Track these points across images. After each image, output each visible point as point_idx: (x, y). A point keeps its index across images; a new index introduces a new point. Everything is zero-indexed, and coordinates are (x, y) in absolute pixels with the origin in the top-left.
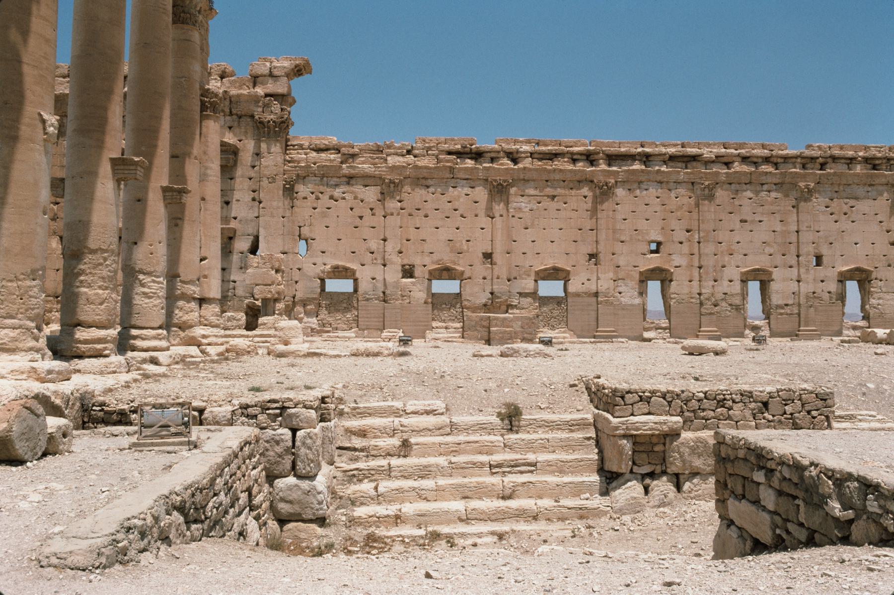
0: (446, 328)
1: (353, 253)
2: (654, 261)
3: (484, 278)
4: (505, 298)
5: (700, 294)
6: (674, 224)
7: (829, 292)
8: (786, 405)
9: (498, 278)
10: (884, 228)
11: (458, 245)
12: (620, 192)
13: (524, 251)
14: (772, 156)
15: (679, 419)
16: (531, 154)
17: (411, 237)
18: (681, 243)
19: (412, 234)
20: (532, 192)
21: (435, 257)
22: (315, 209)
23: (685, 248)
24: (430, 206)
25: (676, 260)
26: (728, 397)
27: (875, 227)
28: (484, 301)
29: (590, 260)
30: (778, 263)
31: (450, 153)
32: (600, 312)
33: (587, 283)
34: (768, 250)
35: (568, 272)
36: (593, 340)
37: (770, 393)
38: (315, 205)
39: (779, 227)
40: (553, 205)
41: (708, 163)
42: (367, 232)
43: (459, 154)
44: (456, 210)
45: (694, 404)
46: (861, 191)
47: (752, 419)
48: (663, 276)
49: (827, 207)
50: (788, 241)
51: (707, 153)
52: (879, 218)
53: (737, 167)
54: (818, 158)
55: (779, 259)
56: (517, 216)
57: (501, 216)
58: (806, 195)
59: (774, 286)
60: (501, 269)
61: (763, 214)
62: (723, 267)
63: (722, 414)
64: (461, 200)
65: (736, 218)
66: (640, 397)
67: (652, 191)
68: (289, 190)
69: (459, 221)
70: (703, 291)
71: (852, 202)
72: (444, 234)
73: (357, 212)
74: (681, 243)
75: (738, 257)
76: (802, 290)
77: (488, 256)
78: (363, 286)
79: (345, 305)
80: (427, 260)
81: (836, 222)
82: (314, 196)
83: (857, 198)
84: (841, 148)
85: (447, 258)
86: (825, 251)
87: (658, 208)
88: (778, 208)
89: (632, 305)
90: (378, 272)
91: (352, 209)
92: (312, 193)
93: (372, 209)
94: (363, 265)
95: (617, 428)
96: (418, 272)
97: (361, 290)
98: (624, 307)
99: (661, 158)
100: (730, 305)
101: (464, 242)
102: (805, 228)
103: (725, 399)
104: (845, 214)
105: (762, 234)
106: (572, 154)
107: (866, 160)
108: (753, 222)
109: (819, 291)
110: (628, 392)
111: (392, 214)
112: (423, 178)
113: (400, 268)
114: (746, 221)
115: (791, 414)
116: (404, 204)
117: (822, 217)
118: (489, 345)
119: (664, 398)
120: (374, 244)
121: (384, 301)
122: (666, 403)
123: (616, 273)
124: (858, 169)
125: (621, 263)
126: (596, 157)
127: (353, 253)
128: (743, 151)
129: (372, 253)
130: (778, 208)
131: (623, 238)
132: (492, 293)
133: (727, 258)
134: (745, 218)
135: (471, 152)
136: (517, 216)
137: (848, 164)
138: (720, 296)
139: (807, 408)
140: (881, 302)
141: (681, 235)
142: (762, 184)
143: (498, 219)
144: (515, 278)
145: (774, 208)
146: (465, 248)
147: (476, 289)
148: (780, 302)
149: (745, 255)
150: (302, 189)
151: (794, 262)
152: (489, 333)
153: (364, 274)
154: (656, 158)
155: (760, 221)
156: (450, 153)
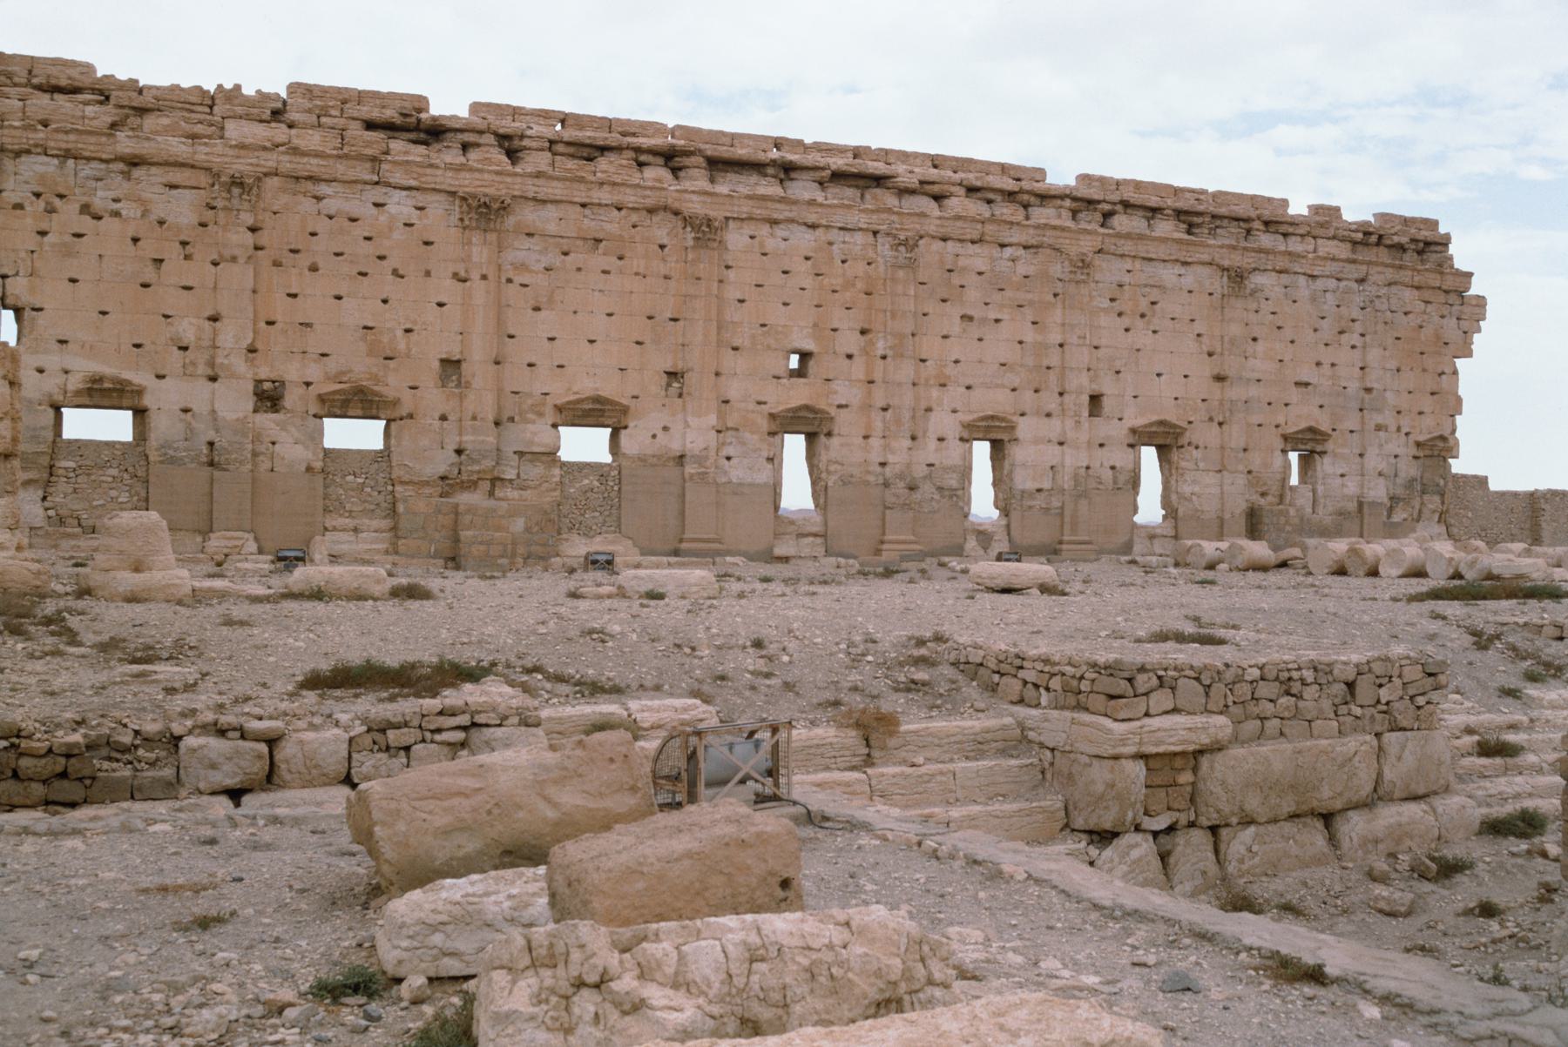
0: (356, 530)
1: (137, 346)
2: (798, 394)
3: (443, 418)
4: (488, 463)
5: (883, 464)
6: (838, 318)
7: (1113, 468)
8: (1381, 686)
9: (474, 418)
10: (1205, 349)
11: (385, 340)
13: (533, 360)
14: (1021, 191)
15: (1221, 720)
16: (551, 142)
17: (278, 317)
18: (850, 357)
19: (280, 308)
21: (332, 365)
22: (43, 233)
23: (858, 369)
24: (322, 246)
25: (841, 390)
26: (1295, 675)
28: (442, 469)
29: (669, 385)
31: (370, 125)
32: (688, 498)
33: (660, 434)
35: (625, 410)
36: (673, 559)
37: (1357, 666)
38: (44, 226)
39: (1030, 336)
40: (599, 260)
41: (904, 192)
42: (173, 300)
44: (381, 258)
45: (1243, 690)
47: (1332, 715)
48: (813, 426)
49: (1112, 300)
50: (1046, 363)
52: (1199, 327)
54: (1099, 202)
56: (518, 279)
57: (484, 277)
59: (1018, 453)
60: (482, 400)
61: (1002, 306)
62: (929, 410)
63: (1287, 708)
64: (396, 235)
66: (1160, 678)
69: (390, 287)
70: (891, 458)
72: (356, 311)
73: (149, 248)
74: (850, 357)
75: (956, 393)
76: (1068, 461)
77: (451, 366)
78: (164, 426)
79: (114, 472)
80: (314, 372)
81: (1127, 330)
82: (41, 204)
85: (360, 367)
86: (1107, 387)
87: (808, 282)
88: (1030, 296)
89: (751, 485)
90: (199, 394)
91: (135, 240)
92: (38, 195)
93: (184, 244)
94: (160, 377)
95: (1123, 741)
96: (291, 398)
97: (154, 440)
98: (738, 489)
99: (818, 175)
100: (940, 489)
101: (400, 333)
102: (1075, 340)
103: (1290, 679)
104: (1143, 316)
105: (999, 347)
106: (638, 150)
107: (1179, 213)
108: (984, 320)
109: (1095, 464)
110: (1142, 669)
111: (234, 259)
112: (310, 178)
113: (250, 387)
114: (971, 318)
115: (1387, 703)
116: (264, 238)
117: (1104, 320)
118: (458, 568)
119: (1197, 679)
120: (188, 328)
121: (211, 464)
122: (1201, 689)
123: (721, 416)
125: (733, 394)
126: (687, 161)
127: (137, 346)
128: (971, 176)
129: (185, 349)
130: (1030, 296)
131: (737, 342)
132: (459, 452)
133: (935, 393)
134: (970, 312)
135: (417, 127)
136: (518, 279)
137: (1148, 219)
139: (1411, 692)
140: (1197, 489)
141: (850, 341)
142: (1003, 246)
143: (476, 284)
144: (512, 419)
145: (1022, 296)
146: (402, 346)
147: (425, 442)
148: (1030, 485)
149: (968, 388)
151: (1052, 403)
152: (457, 540)
153: (164, 397)
154: (805, 175)
155: (997, 321)
156: (370, 125)
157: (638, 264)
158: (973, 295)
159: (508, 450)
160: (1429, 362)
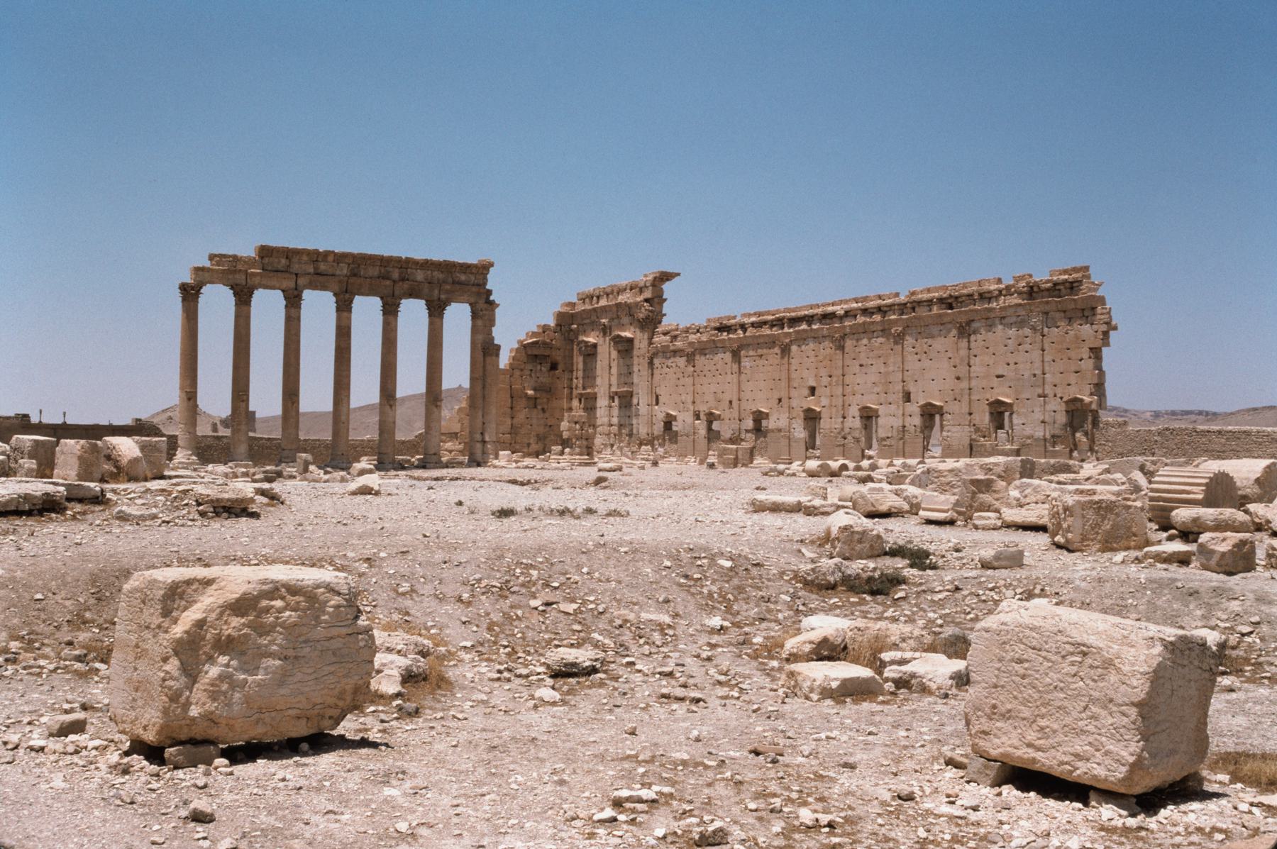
12: (794, 348)
20: (751, 353)
24: (706, 368)
30: (882, 400)
34: (877, 389)
40: (763, 362)
41: (841, 318)
43: (722, 328)
46: (935, 330)
51: (839, 310)
52: (950, 355)
53: (861, 319)
55: (883, 397)
58: (899, 339)
65: (857, 363)
67: (812, 345)
68: (651, 363)
71: (930, 341)
72: (713, 388)
83: (933, 337)
84: (929, 290)
86: (911, 388)
87: (813, 359)
107: (941, 300)
124: (935, 310)
138: (847, 430)
141: (825, 380)
150: (656, 361)
157: (770, 361)
158: (862, 355)
159: (743, 428)
160: (1072, 354)
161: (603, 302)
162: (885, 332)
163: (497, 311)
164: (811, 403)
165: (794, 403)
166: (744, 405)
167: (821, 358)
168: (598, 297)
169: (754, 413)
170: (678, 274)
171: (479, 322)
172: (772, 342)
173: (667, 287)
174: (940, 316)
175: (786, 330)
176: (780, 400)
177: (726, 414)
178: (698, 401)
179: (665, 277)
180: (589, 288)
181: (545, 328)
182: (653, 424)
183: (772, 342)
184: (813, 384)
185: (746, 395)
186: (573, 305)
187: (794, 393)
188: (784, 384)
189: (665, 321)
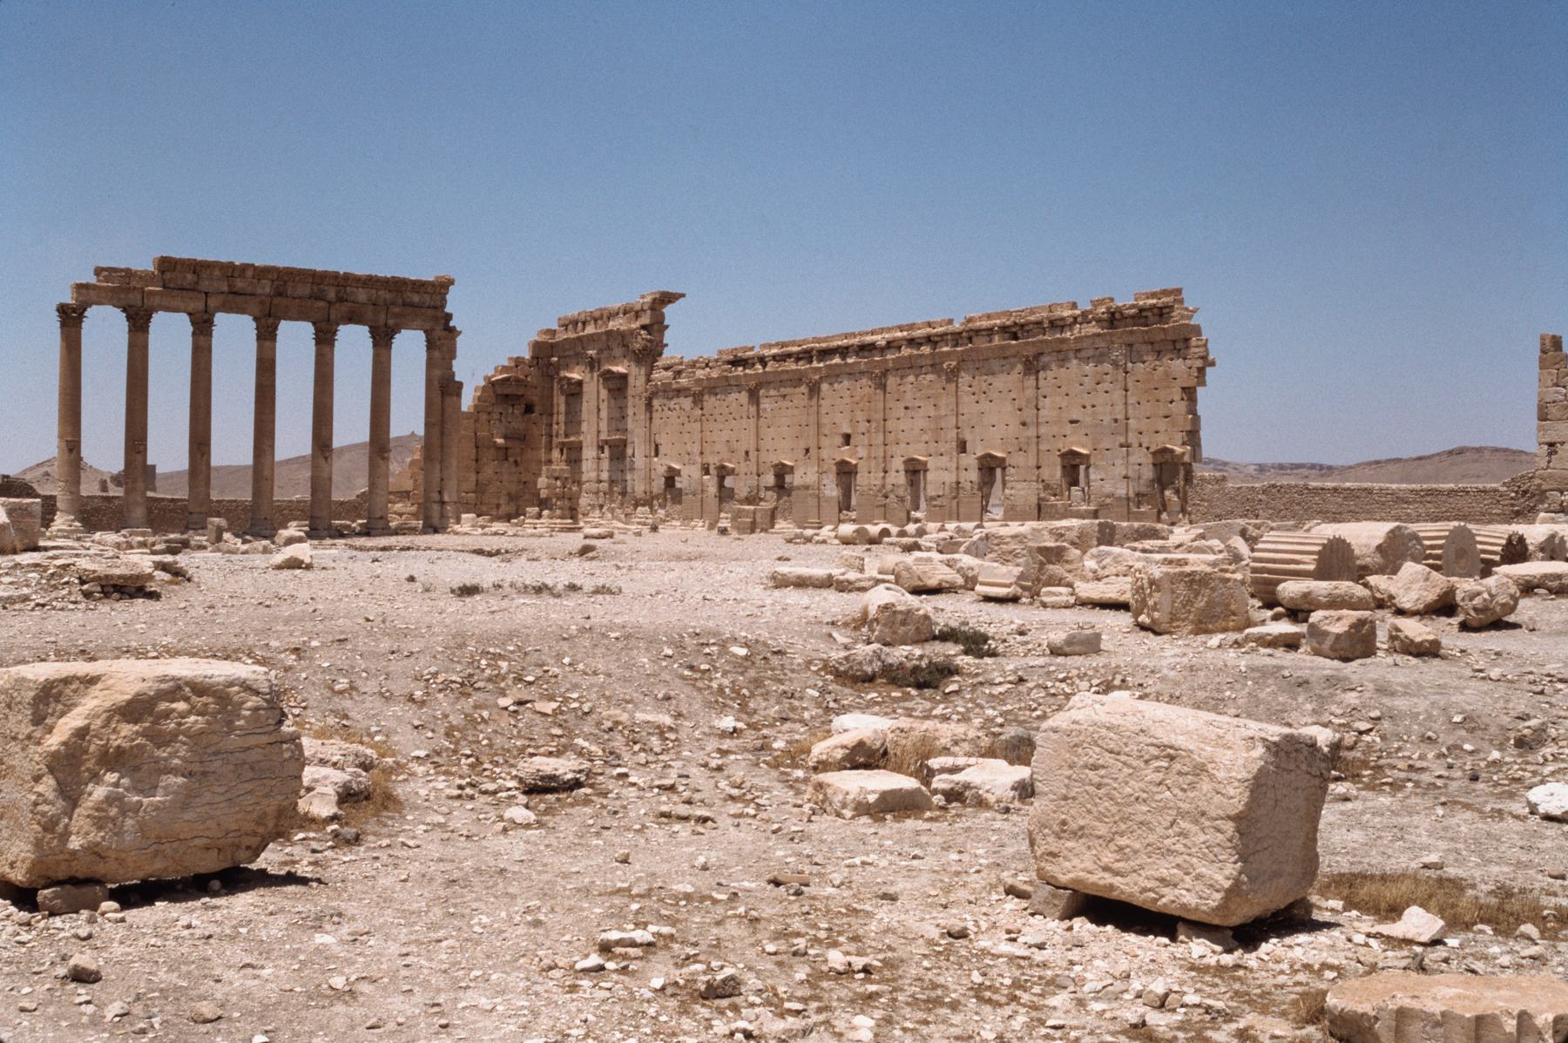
12: (825, 386)
20: (772, 392)
27: (1009, 407)
30: (932, 451)
34: (925, 437)
40: (786, 403)
43: (736, 362)
46: (996, 365)
51: (880, 339)
52: (1013, 395)
53: (906, 351)
58: (953, 375)
65: (901, 405)
67: (846, 383)
68: (649, 406)
71: (990, 379)
72: (726, 435)
84: (989, 317)
86: (968, 436)
87: (847, 400)
124: (997, 340)
138: (889, 487)
141: (863, 426)
150: (656, 403)
158: (909, 395)
160: (1162, 394)
161: (590, 330)
162: (935, 367)
163: (460, 340)
164: (845, 454)
165: (825, 454)
166: (764, 456)
167: (857, 398)
168: (584, 323)
169: (775, 466)
170: (683, 295)
171: (437, 354)
172: (797, 380)
173: (668, 311)
174: (1002, 348)
175: (815, 364)
176: (807, 450)
177: (742, 468)
178: (707, 452)
179: (667, 298)
180: (572, 312)
181: (518, 361)
182: (651, 480)
183: (797, 380)
184: (849, 431)
185: (766, 444)
186: (553, 333)
187: (825, 442)
188: (812, 430)
189: (667, 353)
